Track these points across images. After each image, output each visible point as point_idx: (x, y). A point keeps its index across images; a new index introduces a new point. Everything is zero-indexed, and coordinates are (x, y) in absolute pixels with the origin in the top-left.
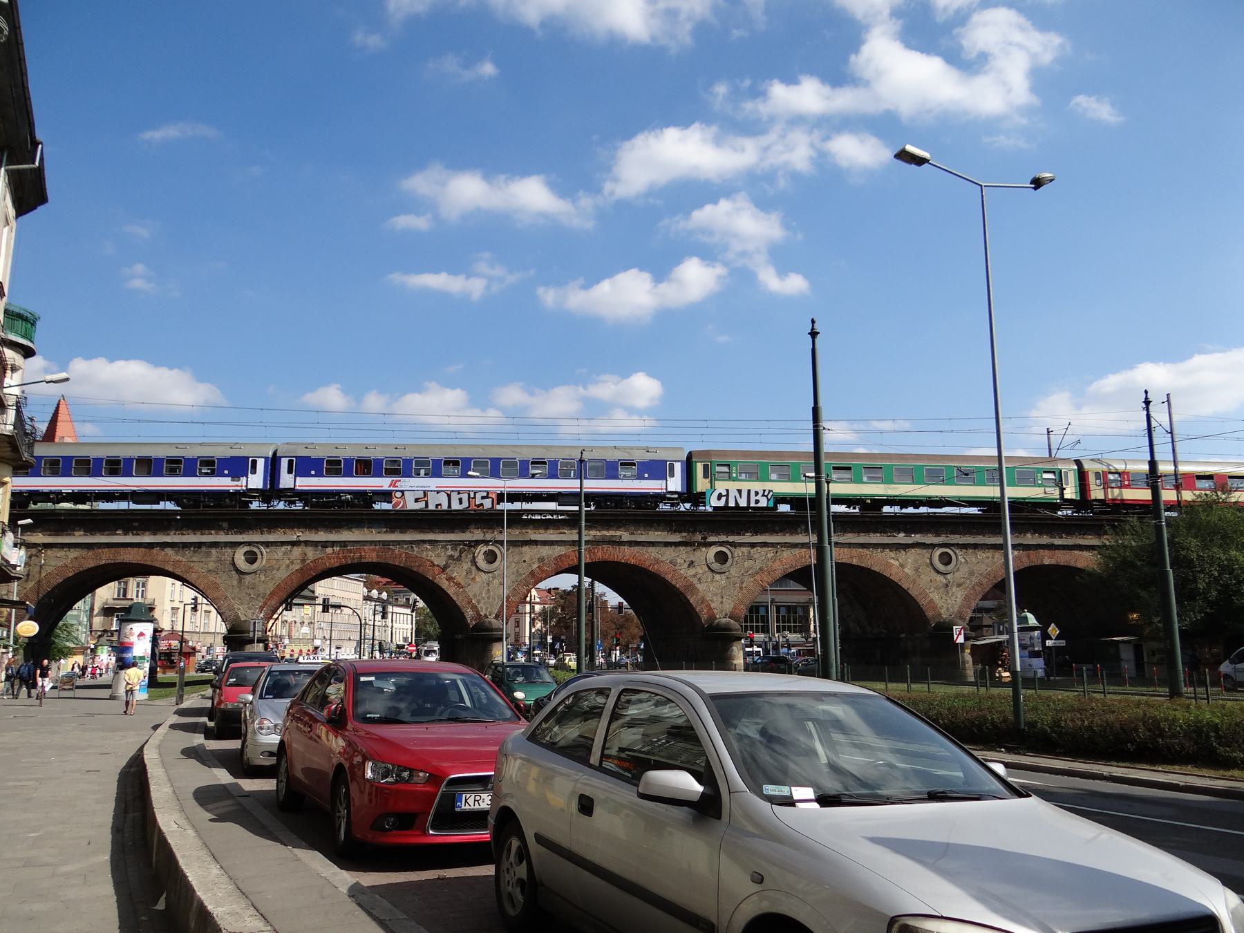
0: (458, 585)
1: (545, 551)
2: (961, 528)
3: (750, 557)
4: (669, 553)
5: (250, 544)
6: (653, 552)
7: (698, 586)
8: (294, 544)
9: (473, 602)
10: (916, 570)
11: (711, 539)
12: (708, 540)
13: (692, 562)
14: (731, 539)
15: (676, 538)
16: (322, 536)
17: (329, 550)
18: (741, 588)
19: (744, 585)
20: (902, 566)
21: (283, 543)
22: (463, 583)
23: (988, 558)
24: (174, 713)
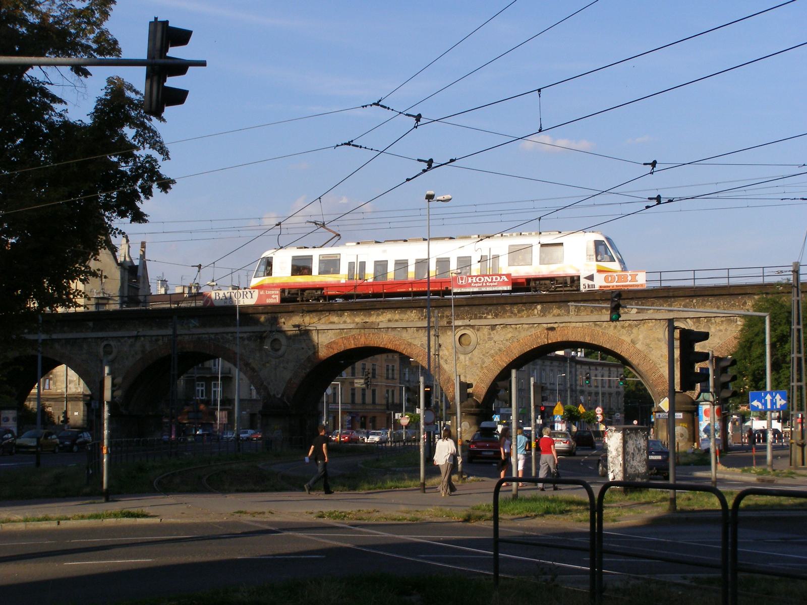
2: (694, 301)
3: (490, 339)
5: (107, 338)
8: (137, 337)
9: (265, 383)
10: (648, 345)
14: (472, 322)
16: (155, 332)
17: (160, 342)
18: (482, 368)
19: (484, 366)
20: (633, 342)
21: (129, 337)
23: (721, 331)
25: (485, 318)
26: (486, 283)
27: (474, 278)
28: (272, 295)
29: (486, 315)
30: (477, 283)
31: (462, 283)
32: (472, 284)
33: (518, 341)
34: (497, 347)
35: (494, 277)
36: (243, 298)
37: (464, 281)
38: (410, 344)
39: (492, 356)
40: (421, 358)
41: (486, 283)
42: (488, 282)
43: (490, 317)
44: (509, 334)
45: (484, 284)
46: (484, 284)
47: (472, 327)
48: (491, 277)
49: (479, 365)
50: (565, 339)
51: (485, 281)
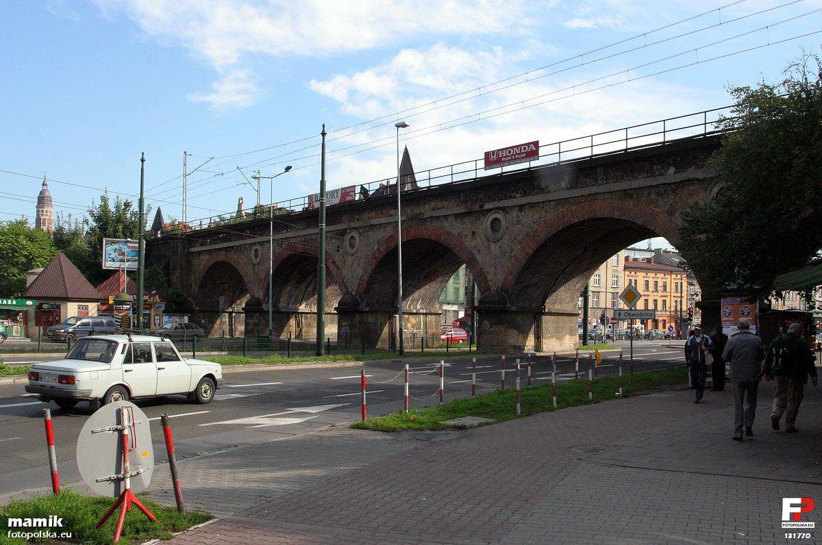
0: (338, 268)
3: (518, 222)
7: (478, 257)
11: (487, 206)
13: (474, 233)
14: (503, 204)
18: (510, 257)
22: (340, 267)
24: (124, 363)
25: (515, 197)
27: (504, 151)
31: (493, 158)
35: (522, 147)
38: (449, 233)
39: (520, 243)
42: (517, 154)
43: (518, 195)
45: (514, 157)
46: (514, 157)
47: (503, 209)
48: (519, 148)
49: (508, 254)
51: (515, 153)
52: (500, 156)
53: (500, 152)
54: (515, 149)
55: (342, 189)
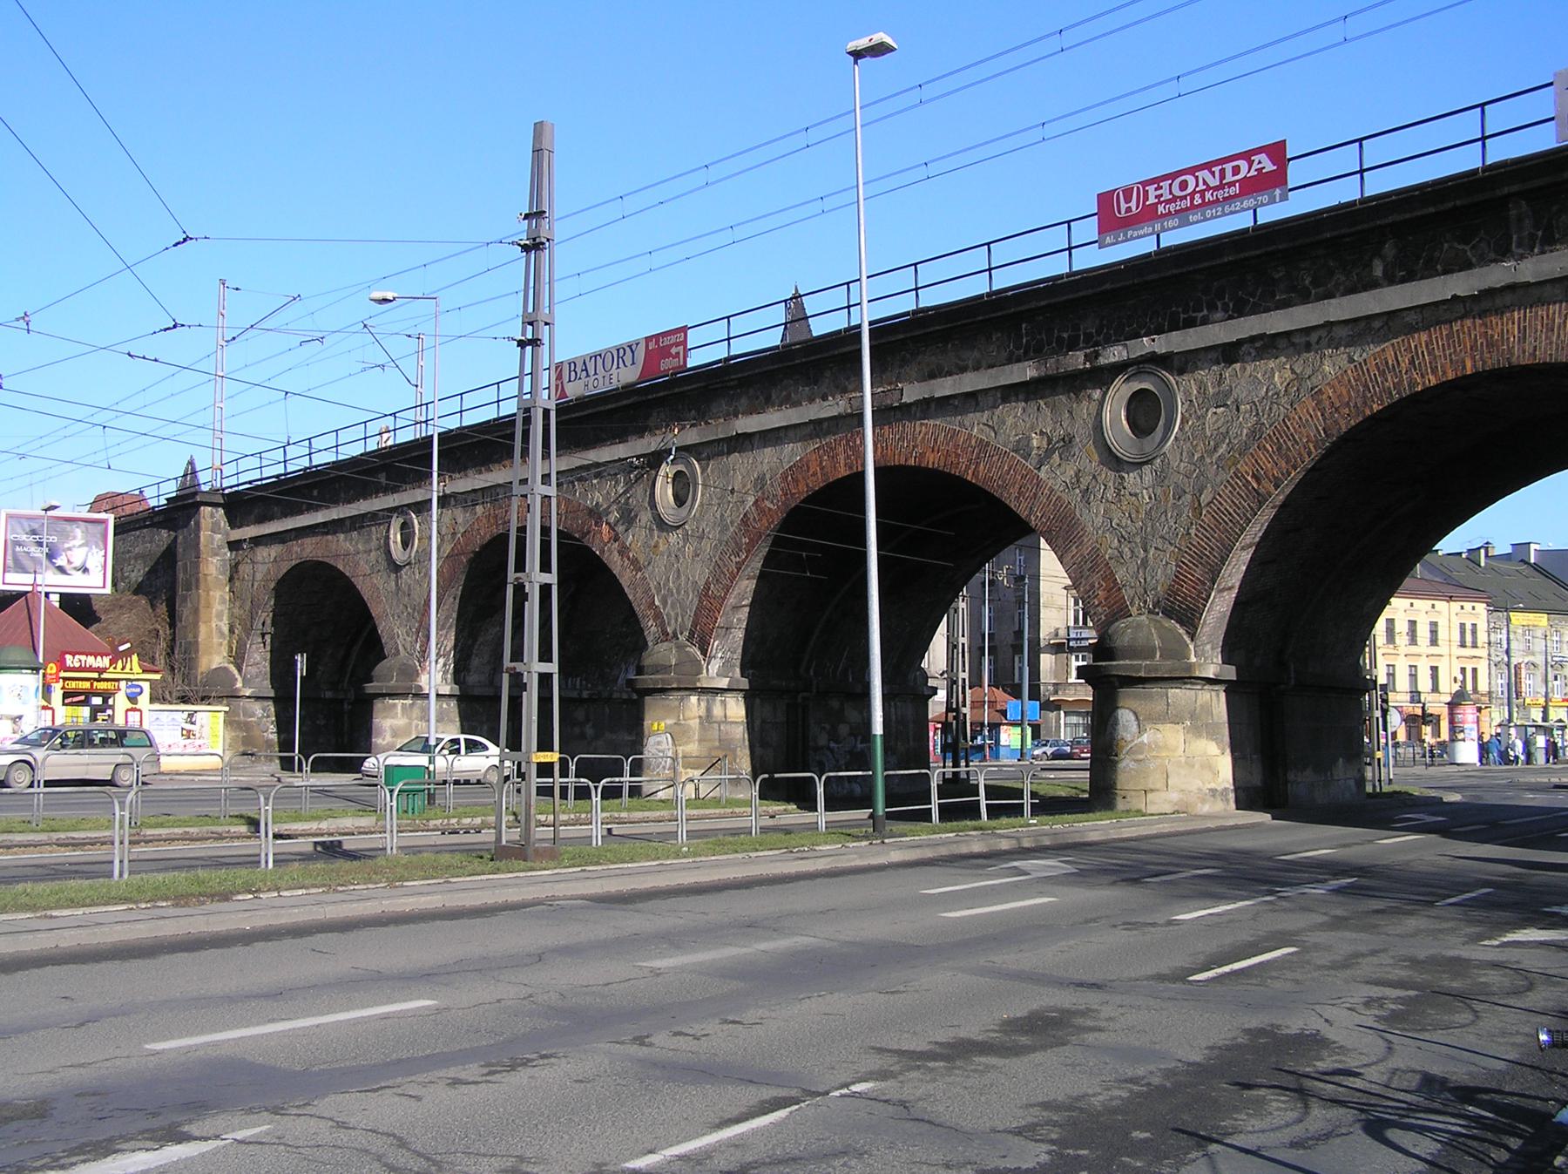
1: (768, 459)
4: (1014, 420)
6: (975, 425)
12: (1102, 361)
15: (1028, 371)
18: (1197, 510)
25: (1205, 321)
26: (1202, 193)
27: (1165, 184)
28: (671, 346)
29: (1205, 312)
30: (1174, 199)
31: (1129, 210)
32: (1160, 209)
33: (1317, 394)
34: (1245, 423)
35: (1228, 167)
36: (618, 367)
37: (1133, 204)
40: (1014, 491)
41: (1202, 193)
42: (1209, 188)
43: (1219, 315)
44: (1278, 372)
45: (1198, 200)
46: (1198, 200)
48: (1216, 169)
50: (1492, 361)
51: (1201, 187)
52: (1152, 200)
53: (1151, 189)
54: (1204, 174)
55: (648, 339)
